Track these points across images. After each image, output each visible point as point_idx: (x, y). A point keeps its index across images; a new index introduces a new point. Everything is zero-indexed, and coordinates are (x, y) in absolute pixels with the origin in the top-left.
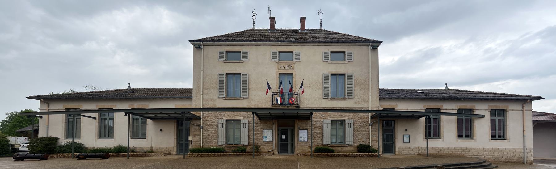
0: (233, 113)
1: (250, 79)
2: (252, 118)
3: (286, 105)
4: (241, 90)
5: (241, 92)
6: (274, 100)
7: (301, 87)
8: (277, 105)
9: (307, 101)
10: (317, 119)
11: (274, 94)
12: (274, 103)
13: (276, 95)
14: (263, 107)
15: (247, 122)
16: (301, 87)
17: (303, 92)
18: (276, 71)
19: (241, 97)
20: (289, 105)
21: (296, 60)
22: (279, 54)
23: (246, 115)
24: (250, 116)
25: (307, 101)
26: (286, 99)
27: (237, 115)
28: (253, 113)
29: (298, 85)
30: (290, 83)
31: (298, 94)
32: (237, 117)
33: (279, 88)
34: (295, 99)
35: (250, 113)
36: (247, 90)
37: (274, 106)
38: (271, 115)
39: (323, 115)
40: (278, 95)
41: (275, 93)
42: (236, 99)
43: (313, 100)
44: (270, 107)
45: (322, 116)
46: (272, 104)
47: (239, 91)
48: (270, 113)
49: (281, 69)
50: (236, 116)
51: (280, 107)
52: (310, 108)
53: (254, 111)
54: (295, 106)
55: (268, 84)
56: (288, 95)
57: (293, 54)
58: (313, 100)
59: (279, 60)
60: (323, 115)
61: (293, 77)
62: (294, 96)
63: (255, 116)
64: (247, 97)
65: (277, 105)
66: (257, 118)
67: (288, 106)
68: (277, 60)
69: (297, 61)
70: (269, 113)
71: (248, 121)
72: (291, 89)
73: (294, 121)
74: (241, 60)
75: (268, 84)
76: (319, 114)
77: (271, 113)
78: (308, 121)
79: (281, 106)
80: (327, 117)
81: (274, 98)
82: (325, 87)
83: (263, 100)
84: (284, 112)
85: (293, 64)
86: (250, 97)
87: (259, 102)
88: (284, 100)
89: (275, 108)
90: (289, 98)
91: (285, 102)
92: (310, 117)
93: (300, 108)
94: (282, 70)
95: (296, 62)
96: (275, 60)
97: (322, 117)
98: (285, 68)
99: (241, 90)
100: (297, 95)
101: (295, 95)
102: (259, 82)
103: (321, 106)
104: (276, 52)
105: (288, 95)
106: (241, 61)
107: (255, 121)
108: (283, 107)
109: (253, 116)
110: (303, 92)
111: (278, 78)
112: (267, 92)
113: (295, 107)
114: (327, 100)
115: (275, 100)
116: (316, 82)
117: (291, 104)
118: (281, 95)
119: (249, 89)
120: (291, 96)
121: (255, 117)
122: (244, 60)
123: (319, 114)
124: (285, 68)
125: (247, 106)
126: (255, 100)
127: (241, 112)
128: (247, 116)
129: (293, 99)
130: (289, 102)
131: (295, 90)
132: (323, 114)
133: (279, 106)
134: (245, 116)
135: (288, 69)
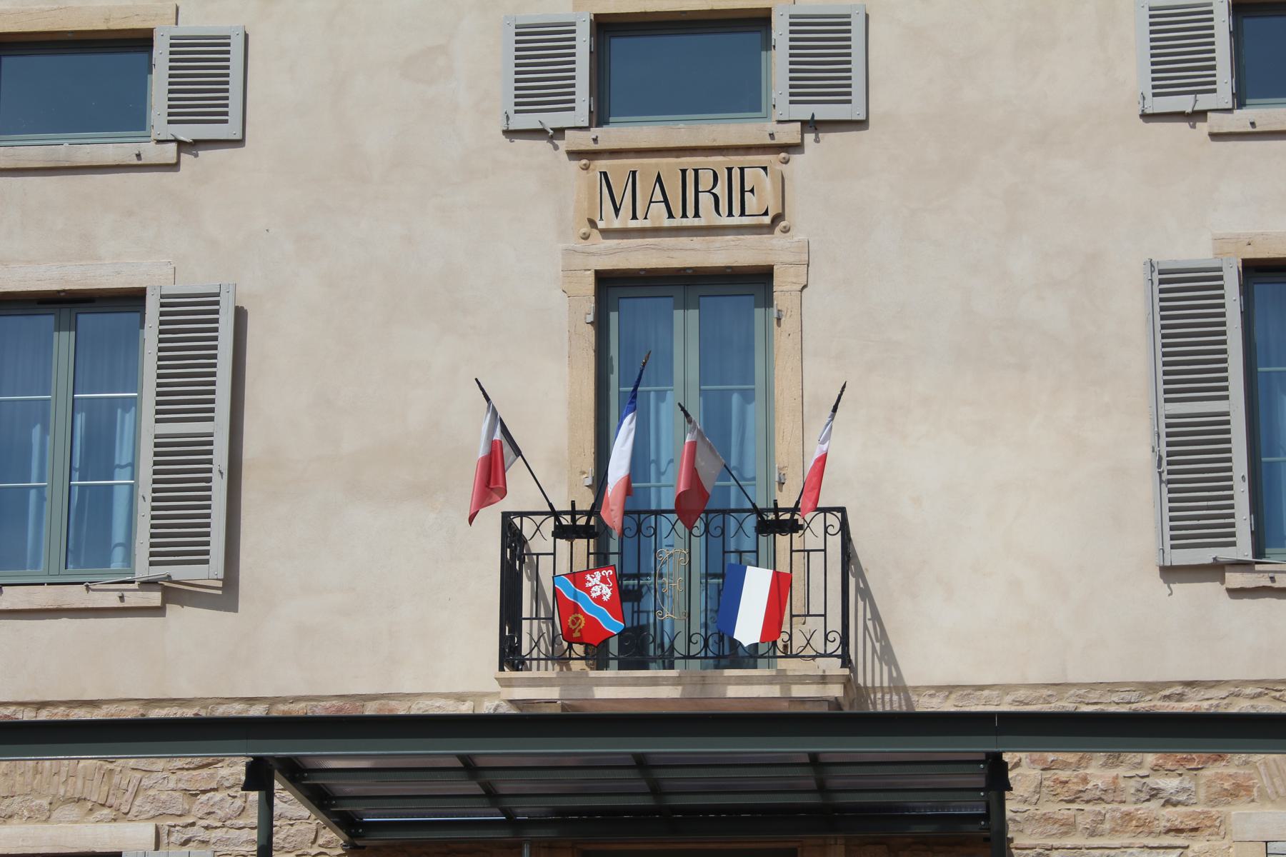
0: (36, 772)
10: (1093, 834)
18: (569, 252)
21: (805, 112)
28: (258, 778)
39: (1169, 784)
45: (1154, 794)
49: (624, 221)
59: (600, 117)
60: (1169, 784)
63: (287, 802)
68: (581, 113)
69: (812, 125)
70: (460, 765)
84: (634, 755)
96: (551, 120)
98: (677, 210)
114: (1211, 590)
121: (293, 821)
122: (187, 132)
124: (677, 209)
132: (1156, 769)
134: (181, 803)
135: (708, 217)
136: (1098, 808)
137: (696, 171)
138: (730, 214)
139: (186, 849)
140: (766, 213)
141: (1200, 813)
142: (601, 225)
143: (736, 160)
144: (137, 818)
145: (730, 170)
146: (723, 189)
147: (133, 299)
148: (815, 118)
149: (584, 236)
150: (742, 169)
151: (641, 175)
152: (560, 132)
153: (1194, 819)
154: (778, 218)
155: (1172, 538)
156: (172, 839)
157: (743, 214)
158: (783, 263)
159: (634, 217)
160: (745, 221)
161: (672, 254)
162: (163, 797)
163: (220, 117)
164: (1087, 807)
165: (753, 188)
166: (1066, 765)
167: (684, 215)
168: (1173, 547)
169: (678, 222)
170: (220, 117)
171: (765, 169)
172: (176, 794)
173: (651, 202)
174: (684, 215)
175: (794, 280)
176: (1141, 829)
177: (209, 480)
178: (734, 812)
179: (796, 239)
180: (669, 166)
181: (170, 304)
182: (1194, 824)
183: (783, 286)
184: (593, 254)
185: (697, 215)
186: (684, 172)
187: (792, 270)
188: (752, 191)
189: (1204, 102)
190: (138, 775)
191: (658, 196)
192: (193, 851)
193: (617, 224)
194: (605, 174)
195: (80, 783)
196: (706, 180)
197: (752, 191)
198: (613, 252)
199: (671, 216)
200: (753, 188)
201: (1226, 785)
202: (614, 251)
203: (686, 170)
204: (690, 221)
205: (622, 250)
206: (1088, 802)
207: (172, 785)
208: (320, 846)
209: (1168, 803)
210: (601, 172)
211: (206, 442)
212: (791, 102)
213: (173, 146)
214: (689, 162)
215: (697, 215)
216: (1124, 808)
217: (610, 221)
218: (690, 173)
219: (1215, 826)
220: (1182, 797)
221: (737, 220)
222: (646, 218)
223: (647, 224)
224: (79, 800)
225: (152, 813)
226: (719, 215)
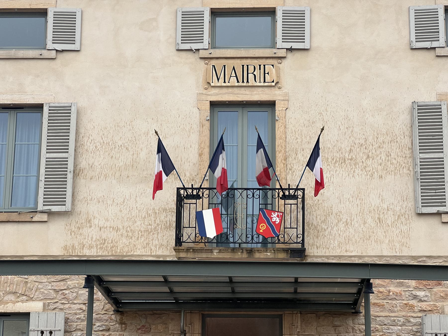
1: (82, 130)
2: (84, 307)
3: (244, 246)
4: (42, 178)
5: (42, 185)
6: (185, 222)
7: (311, 164)
8: (202, 245)
9: (342, 226)
11: (189, 197)
12: (185, 238)
13: (197, 197)
14: (138, 253)
15: (61, 325)
16: (311, 164)
17: (319, 185)
19: (40, 207)
20: (254, 246)
21: (288, 45)
22: (213, 23)
23: (56, 291)
24: (76, 298)
25: (342, 226)
26: (240, 215)
27: (15, 293)
29: (299, 156)
30: (260, 145)
31: (300, 193)
32: (14, 303)
33: (213, 165)
34: (282, 217)
35: (80, 280)
36: (70, 176)
37: (188, 250)
38: (172, 292)
39: (421, 294)
40: (206, 201)
41: (193, 189)
42: (14, 217)
43: (369, 220)
44: (167, 253)
46: (179, 241)
47: (33, 180)
48: (166, 281)
49: (221, 83)
50: (12, 297)
51: (216, 255)
52: (357, 261)
53: (95, 271)
54: (285, 250)
55: (161, 149)
56: (250, 201)
57: (274, 21)
58: (369, 220)
59: (213, 45)
60: (421, 294)
61: (274, 120)
62: (282, 202)
64: (68, 207)
65: (202, 245)
66: (108, 306)
67: (250, 252)
68: (206, 44)
69: (290, 50)
71: (67, 321)
72: (266, 171)
73: (280, 317)
74: (45, 48)
75: (161, 149)
76: (398, 290)
77: (171, 279)
78: (350, 322)
79: (220, 251)
80: (439, 304)
81: (185, 214)
82: (424, 164)
83: (138, 223)
85: (274, 62)
86: (81, 207)
87: (118, 230)
88: (233, 222)
89: (190, 256)
90: (256, 212)
91: (238, 231)
92: (356, 303)
93: (309, 260)
94: (225, 90)
95: (290, 55)
96: (194, 46)
97: (414, 302)
98: (240, 79)
99: (42, 178)
100: (295, 197)
101: (284, 197)
102: (120, 143)
103: (406, 253)
104: (201, 13)
105: (250, 201)
106: (46, 54)
107: (98, 320)
108: (227, 256)
109: (91, 294)
110: (319, 185)
111: (208, 124)
112: (158, 186)
113: (282, 256)
115: (193, 224)
116: (381, 139)
117: (265, 239)
118: (218, 199)
119: (76, 174)
120: (266, 204)
123: (398, 290)
124: (240, 79)
125: (65, 248)
126: (101, 224)
127: (33, 278)
128: (60, 296)
129: (275, 218)
130: (258, 228)
131: (283, 175)
132: (416, 288)
133: (211, 251)
136: (394, 302)
137: (248, 66)
138: (260, 82)
139: (54, 312)
140: (273, 82)
141: (433, 305)
142: (212, 84)
143: (262, 62)
144: (36, 300)
145: (260, 66)
146: (257, 73)
147: (39, 107)
148: (292, 48)
149: (206, 89)
150: (264, 66)
151: (227, 67)
152: (198, 50)
153: (430, 307)
154: (277, 83)
155: (422, 203)
156: (49, 308)
157: (264, 82)
158: (279, 100)
159: (225, 82)
160: (266, 84)
161: (239, 96)
162: (46, 292)
163: (73, 42)
164: (390, 302)
165: (268, 73)
166: (383, 286)
167: (243, 82)
168: (422, 206)
169: (241, 84)
170: (73, 42)
171: (273, 65)
172: (51, 291)
173: (231, 76)
174: (243, 82)
175: (283, 106)
176: (410, 310)
177: (66, 175)
178: (259, 300)
179: (284, 91)
180: (238, 64)
181: (52, 110)
182: (430, 309)
183: (278, 107)
184: (209, 95)
185: (248, 82)
186: (243, 66)
187: (282, 102)
188: (268, 73)
189: (435, 44)
190: (37, 284)
191: (233, 74)
192: (57, 312)
193: (219, 84)
194: (214, 66)
195: (15, 287)
196: (251, 69)
197: (268, 73)
198: (217, 95)
199: (238, 82)
200: (268, 73)
201: (442, 295)
202: (217, 94)
203: (244, 65)
204: (245, 84)
205: (221, 94)
206: (390, 299)
207: (50, 288)
208: (106, 311)
209: (421, 301)
210: (212, 66)
211: (66, 160)
212: (283, 42)
213: (55, 51)
214: (245, 62)
215: (248, 82)
216: (405, 302)
217: (215, 83)
218: (245, 67)
219: (438, 310)
220: (426, 299)
221: (262, 84)
222: (229, 82)
223: (229, 84)
224: (14, 292)
225: (42, 298)
226: (256, 82)
